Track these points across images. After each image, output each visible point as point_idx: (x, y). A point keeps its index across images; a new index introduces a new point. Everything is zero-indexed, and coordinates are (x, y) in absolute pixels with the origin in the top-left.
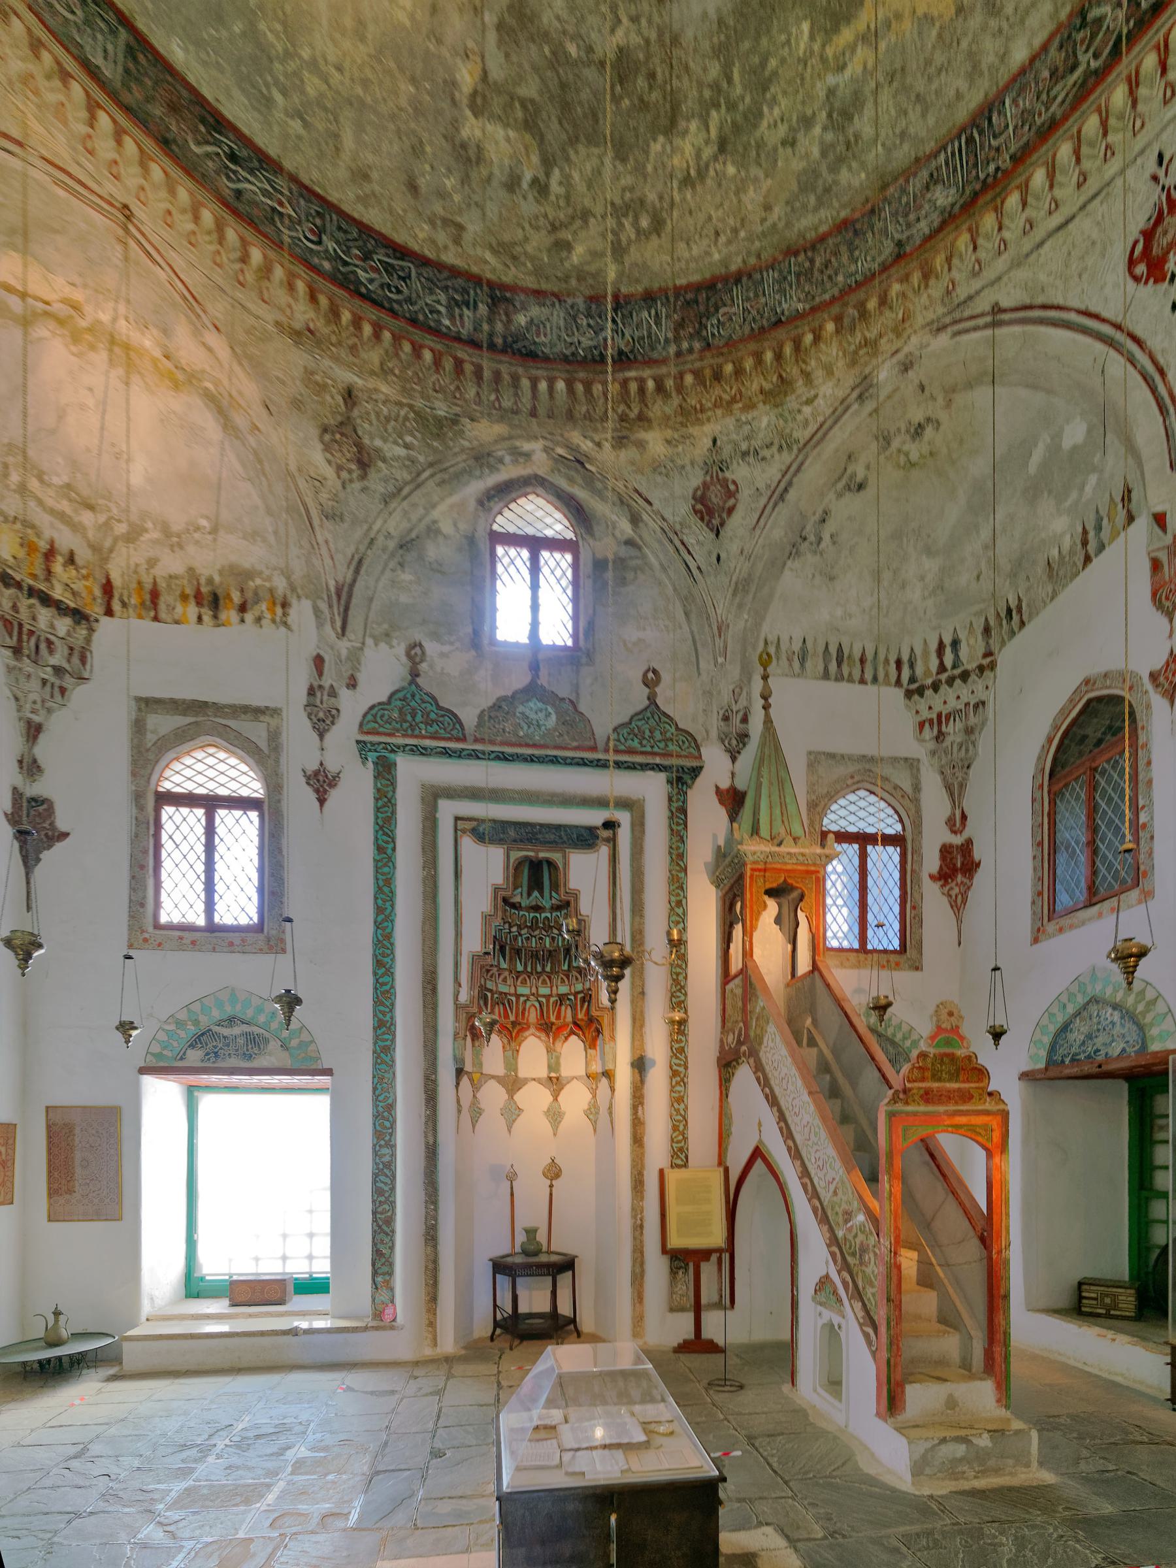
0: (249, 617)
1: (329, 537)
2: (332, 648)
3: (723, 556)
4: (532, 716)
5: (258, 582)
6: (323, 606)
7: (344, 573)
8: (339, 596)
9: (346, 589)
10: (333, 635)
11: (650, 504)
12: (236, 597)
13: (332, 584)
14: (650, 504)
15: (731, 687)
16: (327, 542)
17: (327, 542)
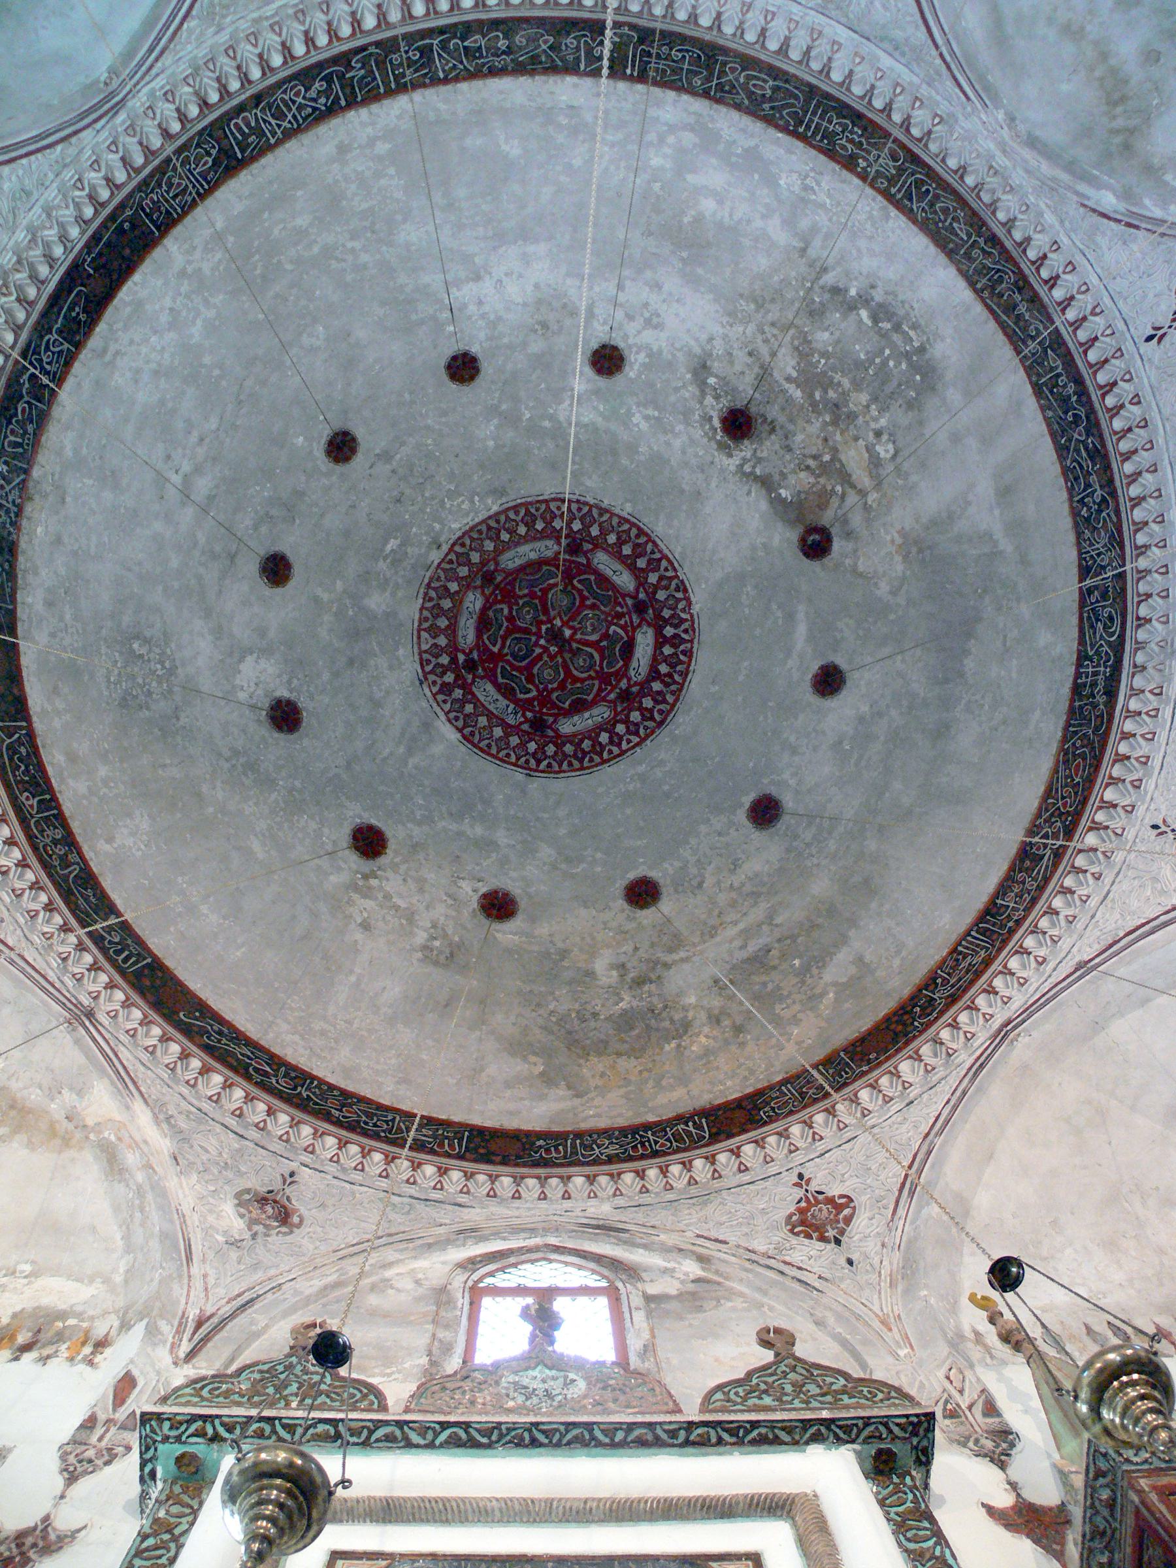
0: (28, 1357)
1: (212, 1273)
2: (158, 1373)
3: (854, 1258)
4: (534, 1385)
5: (71, 1322)
6: (167, 1329)
7: (217, 1303)
8: (199, 1324)
9: (215, 1320)
10: (169, 1360)
11: (725, 1242)
12: (21, 1339)
13: (193, 1314)
14: (725, 1242)
15: (941, 1374)
16: (205, 1276)
17: (205, 1276)
